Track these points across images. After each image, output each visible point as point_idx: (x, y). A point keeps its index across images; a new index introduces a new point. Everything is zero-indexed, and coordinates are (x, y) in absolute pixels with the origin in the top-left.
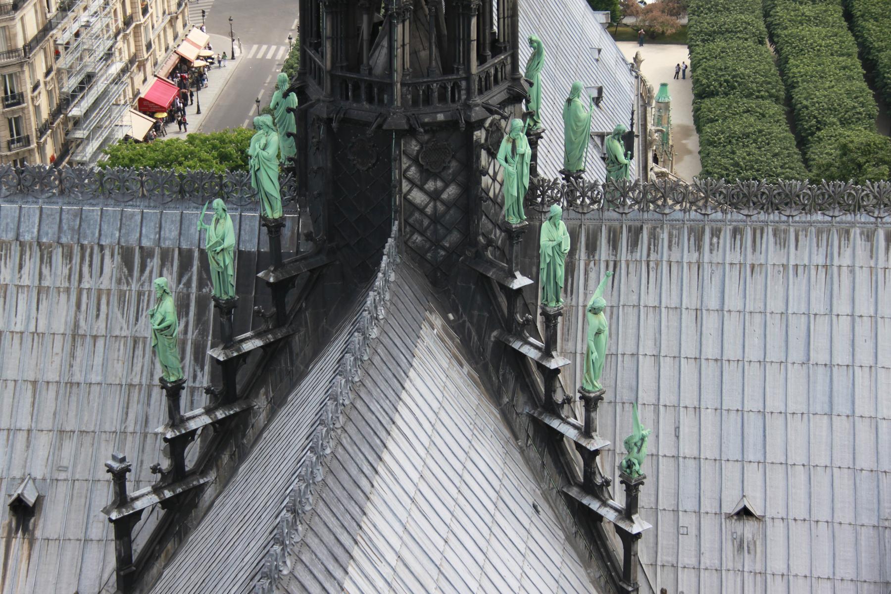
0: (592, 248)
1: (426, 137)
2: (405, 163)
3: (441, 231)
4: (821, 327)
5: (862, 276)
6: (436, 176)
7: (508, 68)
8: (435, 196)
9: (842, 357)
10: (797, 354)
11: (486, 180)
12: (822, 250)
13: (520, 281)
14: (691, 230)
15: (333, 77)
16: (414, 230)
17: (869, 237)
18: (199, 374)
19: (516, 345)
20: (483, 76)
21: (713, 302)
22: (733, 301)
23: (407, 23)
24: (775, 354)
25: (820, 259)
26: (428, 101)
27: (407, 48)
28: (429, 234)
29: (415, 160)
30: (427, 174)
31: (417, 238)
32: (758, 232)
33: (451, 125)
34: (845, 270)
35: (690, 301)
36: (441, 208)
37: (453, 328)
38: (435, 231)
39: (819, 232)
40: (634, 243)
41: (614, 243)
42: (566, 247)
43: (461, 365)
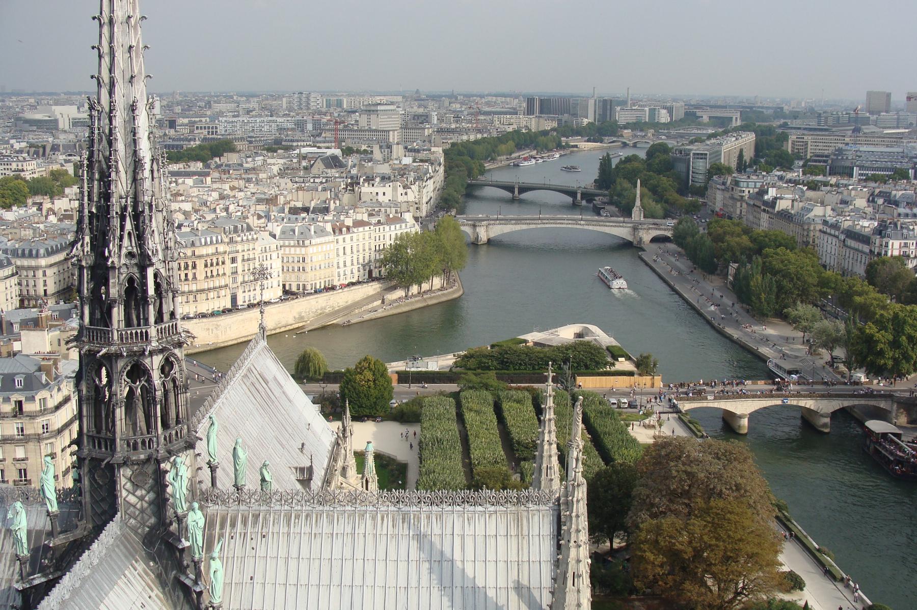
0: (233, 525)
1: (136, 467)
2: (123, 481)
3: (146, 517)
4: (348, 565)
5: (370, 539)
6: (141, 488)
7: (185, 431)
8: (141, 498)
9: (358, 581)
10: (336, 581)
11: (169, 490)
12: (350, 526)
13: (186, 544)
14: (285, 516)
15: (88, 436)
16: (131, 517)
17: (374, 518)
18: (17, 598)
19: (183, 578)
20: (167, 435)
21: (295, 555)
22: (305, 553)
23: (123, 408)
24: (325, 580)
25: (349, 529)
26: (135, 448)
27: (124, 421)
28: (139, 519)
29: (130, 479)
30: (136, 486)
31: (132, 521)
32: (319, 515)
33: (148, 460)
34: (361, 536)
35: (282, 553)
36: (145, 505)
37: (151, 570)
38: (143, 518)
39: (349, 516)
40: (255, 522)
41: (245, 522)
42: (201, 523)
43: (152, 590)
